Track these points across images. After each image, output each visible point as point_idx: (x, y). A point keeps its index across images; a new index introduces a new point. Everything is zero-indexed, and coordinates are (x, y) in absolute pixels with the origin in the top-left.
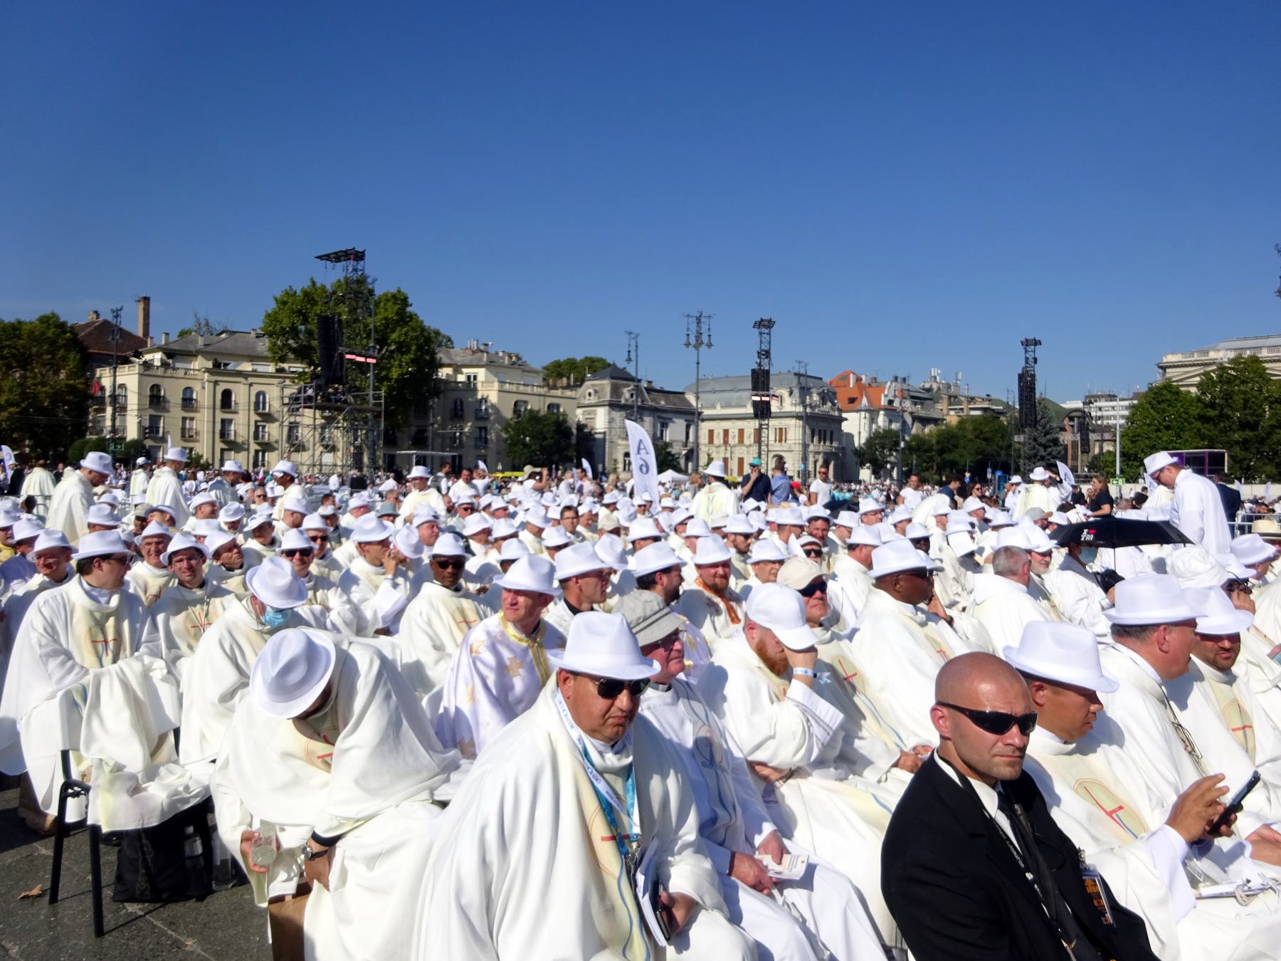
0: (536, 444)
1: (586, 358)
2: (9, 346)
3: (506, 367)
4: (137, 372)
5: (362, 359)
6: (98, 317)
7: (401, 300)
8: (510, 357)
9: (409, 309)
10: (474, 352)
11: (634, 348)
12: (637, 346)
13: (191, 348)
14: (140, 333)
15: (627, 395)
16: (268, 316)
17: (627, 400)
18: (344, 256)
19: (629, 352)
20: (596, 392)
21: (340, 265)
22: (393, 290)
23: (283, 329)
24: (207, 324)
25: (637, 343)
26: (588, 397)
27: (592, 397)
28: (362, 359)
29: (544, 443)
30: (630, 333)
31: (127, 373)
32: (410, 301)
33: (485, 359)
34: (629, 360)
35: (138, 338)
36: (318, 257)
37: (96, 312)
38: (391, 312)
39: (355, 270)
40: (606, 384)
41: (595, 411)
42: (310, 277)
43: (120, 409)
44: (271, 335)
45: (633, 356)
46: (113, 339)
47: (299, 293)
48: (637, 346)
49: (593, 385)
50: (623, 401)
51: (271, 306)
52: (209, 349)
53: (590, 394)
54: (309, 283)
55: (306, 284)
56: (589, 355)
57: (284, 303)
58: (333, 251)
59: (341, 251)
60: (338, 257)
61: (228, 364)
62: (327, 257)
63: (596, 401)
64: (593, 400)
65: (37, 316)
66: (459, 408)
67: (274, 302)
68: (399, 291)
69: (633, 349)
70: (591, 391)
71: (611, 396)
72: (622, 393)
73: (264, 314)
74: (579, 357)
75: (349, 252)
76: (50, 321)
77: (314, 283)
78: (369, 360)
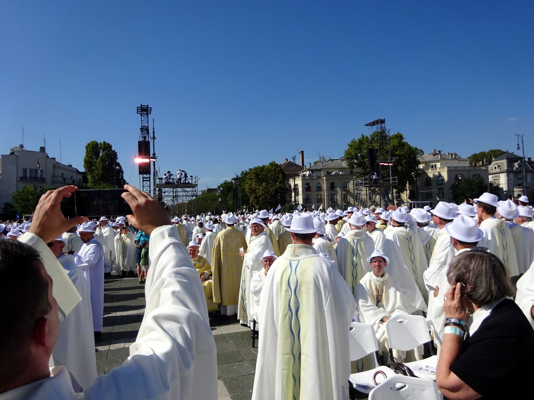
0: (469, 194)
1: (491, 151)
2: (261, 175)
3: (450, 160)
4: (301, 179)
5: (387, 164)
6: (287, 161)
7: (400, 137)
8: (452, 155)
9: (403, 140)
10: (434, 155)
11: (521, 142)
12: (523, 141)
13: (319, 168)
14: (301, 165)
15: (517, 166)
16: (346, 152)
17: (516, 168)
18: (376, 123)
19: (518, 145)
20: (499, 166)
21: (375, 127)
22: (396, 133)
23: (352, 156)
24: (323, 158)
25: (522, 140)
26: (494, 169)
27: (497, 169)
28: (387, 164)
29: (473, 193)
30: (518, 135)
31: (298, 180)
32: (403, 137)
33: (440, 158)
34: (519, 148)
35: (301, 166)
36: (366, 125)
37: (287, 159)
38: (395, 142)
39: (381, 128)
40: (504, 163)
41: (499, 175)
42: (361, 134)
43: (297, 194)
44: (347, 159)
45: (521, 146)
46: (293, 168)
47: (357, 141)
48: (523, 141)
49: (496, 164)
50: (515, 170)
51: (347, 147)
52: (325, 168)
53: (495, 168)
54: (361, 136)
55: (360, 137)
56: (492, 149)
57: (352, 146)
58: (372, 122)
59: (375, 121)
60: (373, 124)
61: (332, 173)
62: (370, 124)
63: (500, 171)
64: (498, 170)
65: (269, 163)
66: (429, 180)
67: (348, 146)
68: (398, 133)
69: (520, 143)
70: (496, 166)
71: (508, 167)
72: (514, 165)
73: (344, 151)
74: (487, 151)
75: (378, 121)
76: (273, 164)
77: (363, 136)
78: (390, 164)
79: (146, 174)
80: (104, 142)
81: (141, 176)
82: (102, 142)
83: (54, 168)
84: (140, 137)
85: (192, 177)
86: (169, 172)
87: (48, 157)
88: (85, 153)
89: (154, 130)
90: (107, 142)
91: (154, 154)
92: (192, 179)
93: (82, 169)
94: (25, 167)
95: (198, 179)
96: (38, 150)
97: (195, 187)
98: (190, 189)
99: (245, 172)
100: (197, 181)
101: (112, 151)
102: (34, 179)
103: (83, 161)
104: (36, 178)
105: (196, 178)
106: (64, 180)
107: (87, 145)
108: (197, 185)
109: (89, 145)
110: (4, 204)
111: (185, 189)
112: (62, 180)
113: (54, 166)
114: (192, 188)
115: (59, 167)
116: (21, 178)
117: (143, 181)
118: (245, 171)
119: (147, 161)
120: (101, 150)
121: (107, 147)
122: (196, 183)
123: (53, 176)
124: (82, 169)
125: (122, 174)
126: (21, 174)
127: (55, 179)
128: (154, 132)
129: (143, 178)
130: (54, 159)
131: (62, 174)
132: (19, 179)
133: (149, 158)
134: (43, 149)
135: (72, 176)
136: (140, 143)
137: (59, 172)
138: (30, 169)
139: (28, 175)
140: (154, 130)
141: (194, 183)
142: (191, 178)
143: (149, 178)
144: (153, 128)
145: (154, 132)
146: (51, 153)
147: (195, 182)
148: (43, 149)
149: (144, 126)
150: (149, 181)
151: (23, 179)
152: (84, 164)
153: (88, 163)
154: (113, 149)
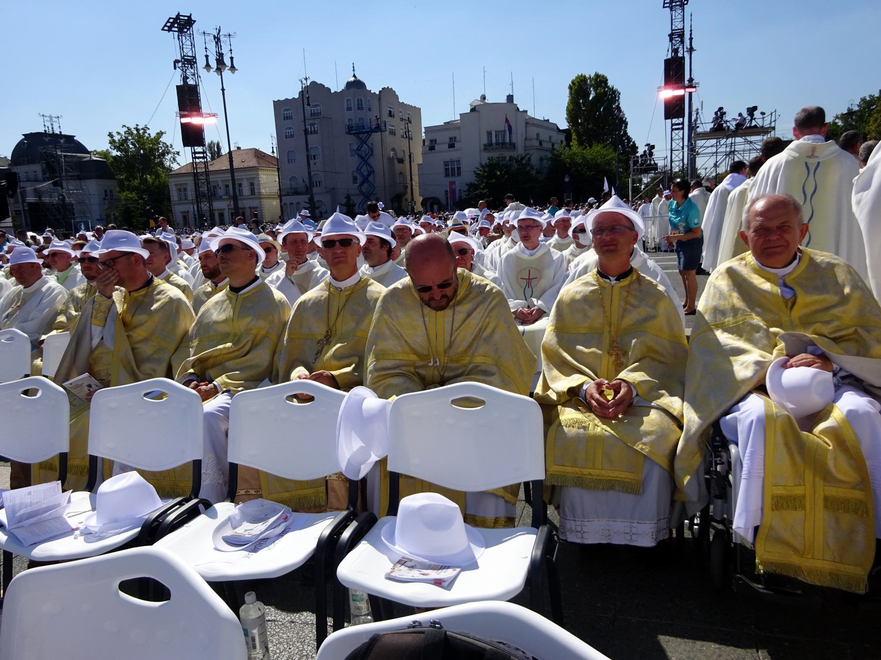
79: (678, 118)
80: (597, 76)
81: (669, 121)
82: (592, 75)
83: (526, 127)
84: (668, 51)
85: (763, 114)
86: (721, 109)
87: (518, 109)
88: (568, 98)
89: (691, 34)
90: (601, 73)
91: (691, 80)
92: (763, 118)
93: (564, 125)
94: (489, 129)
95: (777, 116)
96: (503, 100)
97: (771, 132)
98: (759, 138)
99: (868, 99)
100: (775, 121)
101: (608, 87)
102: (501, 146)
103: (565, 112)
104: (504, 143)
105: (774, 114)
106: (541, 143)
107: (570, 83)
108: (774, 128)
109: (573, 82)
110: (467, 185)
111: (749, 138)
112: (537, 144)
113: (527, 123)
114: (763, 136)
115: (533, 124)
116: (485, 145)
117: (672, 130)
118: (870, 96)
119: (680, 92)
120: (591, 89)
121: (600, 81)
122: (773, 125)
123: (526, 139)
124: (564, 125)
125: (626, 127)
126: (485, 141)
127: (528, 143)
128: (691, 39)
129: (672, 125)
130: (526, 112)
131: (538, 135)
132: (482, 147)
133: (685, 88)
134: (510, 98)
135: (550, 137)
136: (667, 62)
137: (533, 131)
138: (496, 132)
139: (494, 141)
140: (691, 34)
141: (768, 126)
142: (761, 116)
143: (683, 123)
144: (691, 31)
145: (691, 39)
146: (521, 103)
147: (771, 123)
148: (510, 98)
149: (676, 28)
150: (683, 128)
151: (488, 147)
152: (566, 116)
153: (573, 114)
154: (610, 83)
